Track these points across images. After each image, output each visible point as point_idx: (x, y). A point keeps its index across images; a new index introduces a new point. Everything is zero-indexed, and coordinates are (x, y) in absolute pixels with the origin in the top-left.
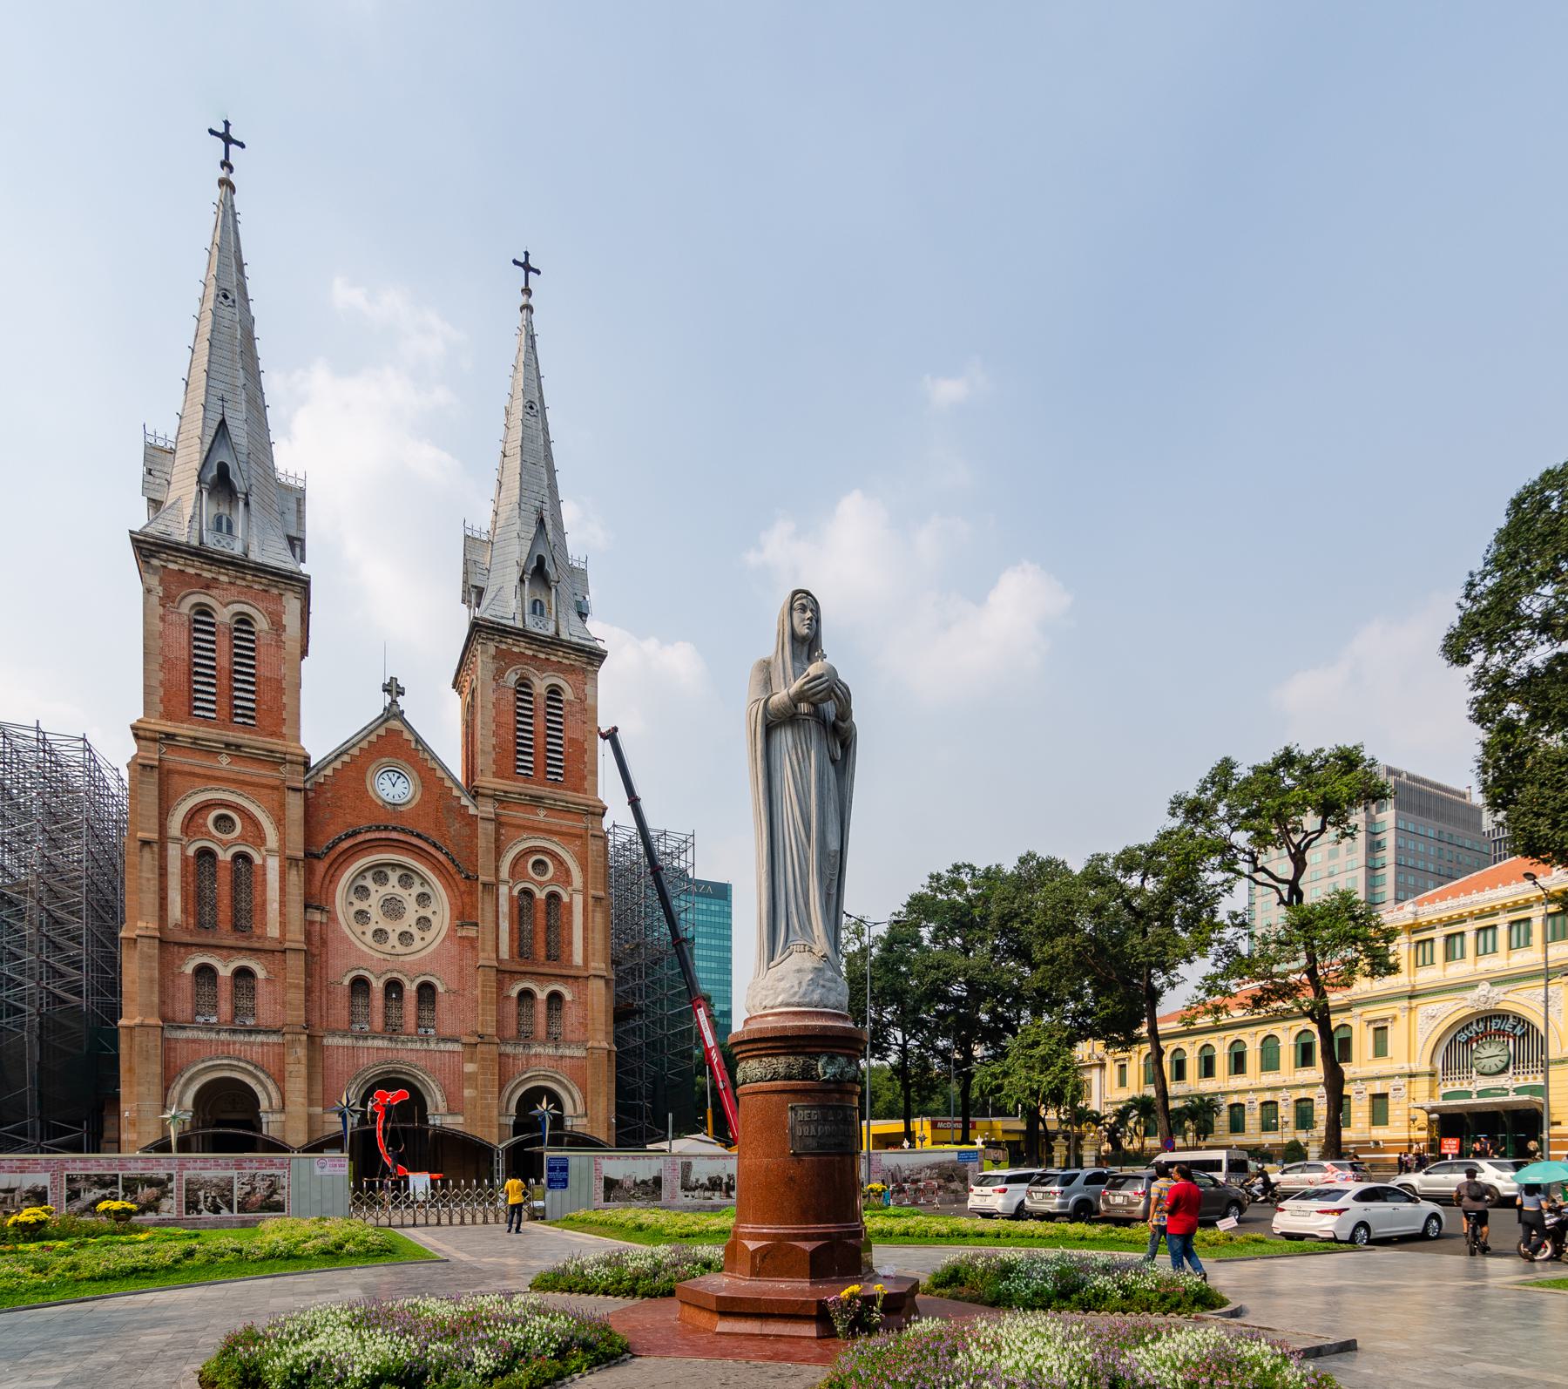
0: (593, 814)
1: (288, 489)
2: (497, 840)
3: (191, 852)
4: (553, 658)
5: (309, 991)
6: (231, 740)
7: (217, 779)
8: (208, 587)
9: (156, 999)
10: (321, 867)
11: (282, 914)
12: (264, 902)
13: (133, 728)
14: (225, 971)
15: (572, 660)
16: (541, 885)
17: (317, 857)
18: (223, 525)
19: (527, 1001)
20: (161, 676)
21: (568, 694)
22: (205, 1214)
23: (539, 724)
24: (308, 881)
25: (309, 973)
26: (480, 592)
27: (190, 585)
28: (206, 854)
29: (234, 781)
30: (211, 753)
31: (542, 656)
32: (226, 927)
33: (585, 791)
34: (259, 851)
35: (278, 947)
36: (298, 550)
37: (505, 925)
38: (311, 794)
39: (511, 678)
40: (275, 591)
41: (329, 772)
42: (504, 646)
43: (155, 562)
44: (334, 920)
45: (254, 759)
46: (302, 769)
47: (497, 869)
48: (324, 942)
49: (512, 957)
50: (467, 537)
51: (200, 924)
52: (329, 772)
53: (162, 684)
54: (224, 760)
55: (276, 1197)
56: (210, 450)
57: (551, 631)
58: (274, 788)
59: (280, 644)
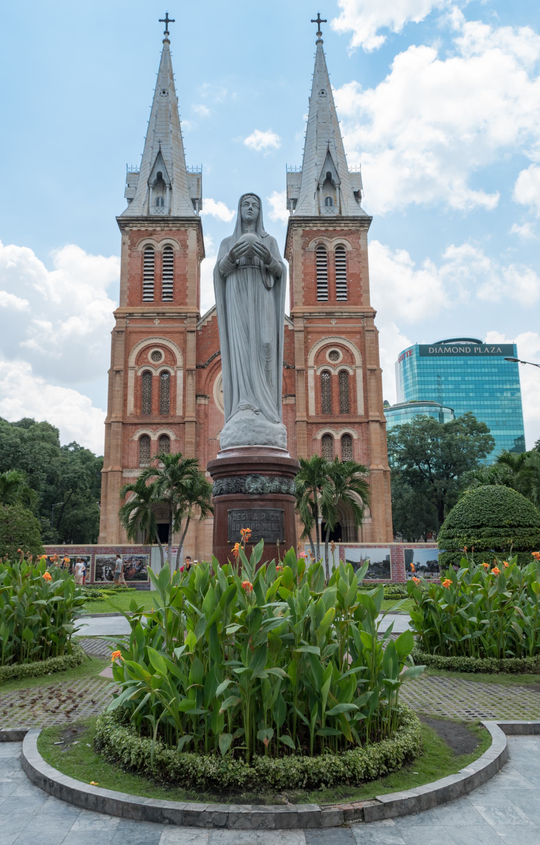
0: (367, 317)
1: (193, 175)
2: (306, 342)
3: (139, 373)
4: (338, 229)
5: (198, 445)
6: (160, 311)
7: (152, 332)
8: (151, 235)
9: (119, 456)
10: (205, 372)
11: (184, 402)
12: (175, 396)
13: (114, 313)
14: (154, 437)
15: (352, 227)
16: (334, 366)
17: (203, 367)
18: (160, 202)
19: (328, 441)
20: (128, 284)
21: (349, 247)
22: (106, 581)
23: (332, 269)
24: (198, 382)
25: (198, 435)
26: (295, 201)
27: (143, 236)
28: (147, 373)
29: (161, 332)
30: (151, 319)
31: (331, 229)
32: (155, 413)
33: (362, 304)
34: (173, 369)
35: (181, 421)
36: (197, 205)
37: (312, 394)
38: (200, 333)
39: (312, 245)
40: (183, 229)
41: (210, 319)
42: (308, 229)
43: (127, 229)
44: (212, 402)
45: (172, 319)
46: (195, 320)
47: (306, 361)
48: (206, 416)
49: (317, 414)
50: (288, 173)
51: (143, 412)
52: (210, 319)
53: (128, 289)
54: (157, 322)
55: (143, 571)
56: (153, 168)
57: (336, 213)
58: (181, 333)
59: (185, 255)
